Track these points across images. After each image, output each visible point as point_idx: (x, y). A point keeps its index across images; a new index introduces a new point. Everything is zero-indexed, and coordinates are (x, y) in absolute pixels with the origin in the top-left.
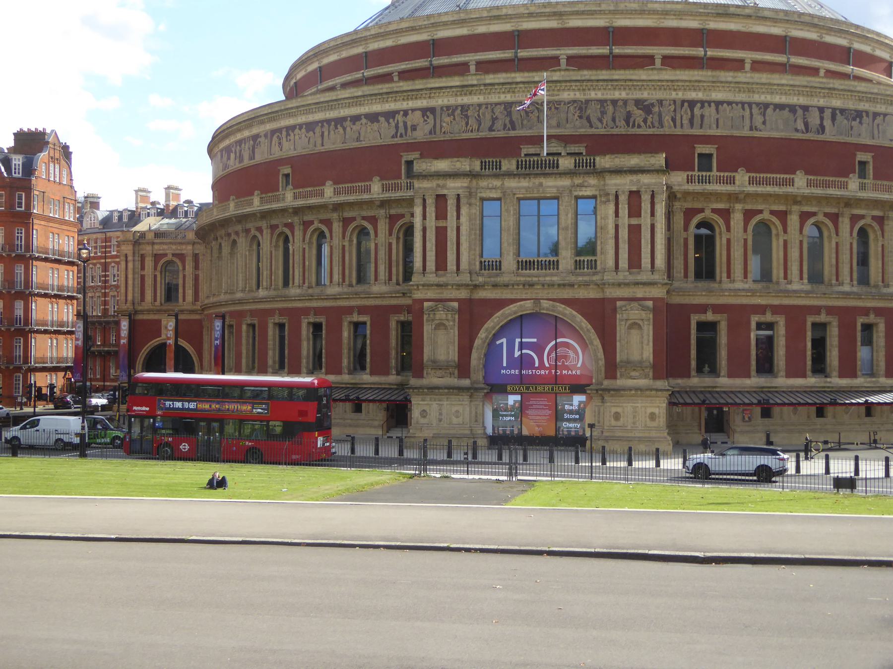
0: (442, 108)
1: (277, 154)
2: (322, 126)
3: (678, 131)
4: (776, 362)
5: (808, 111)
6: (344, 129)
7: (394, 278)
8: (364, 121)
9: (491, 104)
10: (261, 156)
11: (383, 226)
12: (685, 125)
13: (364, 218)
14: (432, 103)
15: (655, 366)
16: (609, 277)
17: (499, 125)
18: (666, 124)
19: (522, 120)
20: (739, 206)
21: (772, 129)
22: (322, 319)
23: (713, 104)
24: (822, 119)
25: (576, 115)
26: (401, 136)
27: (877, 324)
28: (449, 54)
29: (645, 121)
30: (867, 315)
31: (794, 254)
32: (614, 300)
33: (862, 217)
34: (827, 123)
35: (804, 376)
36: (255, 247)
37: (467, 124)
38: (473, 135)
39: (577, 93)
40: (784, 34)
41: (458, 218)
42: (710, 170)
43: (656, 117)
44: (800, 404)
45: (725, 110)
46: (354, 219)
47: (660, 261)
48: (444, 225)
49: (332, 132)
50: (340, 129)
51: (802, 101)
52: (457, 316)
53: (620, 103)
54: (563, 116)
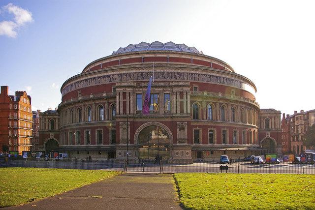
11: (106, 105)
14: (121, 72)
20: (204, 100)
32: (176, 122)
34: (225, 81)
35: (221, 144)
41: (130, 99)
47: (189, 111)
51: (219, 75)
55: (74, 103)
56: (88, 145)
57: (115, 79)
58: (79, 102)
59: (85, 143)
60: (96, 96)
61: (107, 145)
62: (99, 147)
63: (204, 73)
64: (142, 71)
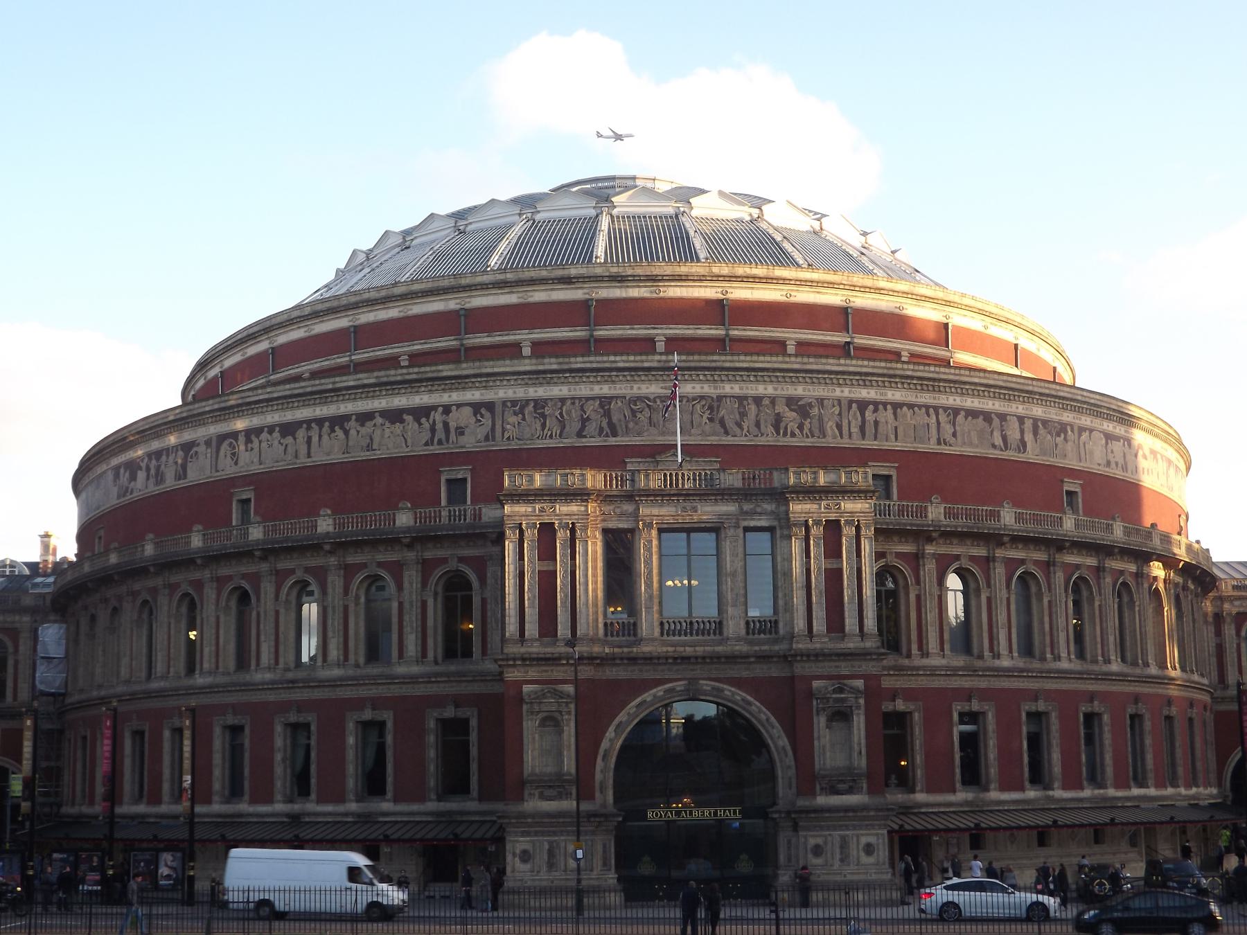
0: (504, 403)
1: (228, 469)
2: (309, 428)
3: (845, 443)
4: (983, 771)
5: (1006, 420)
6: (346, 433)
7: (431, 654)
8: (379, 420)
9: (580, 399)
10: (199, 472)
11: (412, 577)
12: (854, 436)
13: (380, 564)
15: (870, 776)
16: (801, 646)
17: (591, 428)
18: (829, 432)
19: (627, 422)
20: (930, 549)
21: (964, 443)
22: (311, 718)
23: (889, 407)
24: (1022, 432)
26: (440, 442)
27: (1099, 715)
28: (489, 330)
29: (801, 427)
30: (1091, 701)
31: (1002, 617)
32: (809, 679)
33: (1078, 567)
34: (1029, 437)
35: (1022, 789)
36: (184, 610)
37: (544, 426)
38: (552, 443)
39: (706, 386)
40: (945, 321)
42: (888, 496)
43: (815, 421)
44: (1019, 828)
45: (905, 416)
46: (364, 566)
48: (551, 568)
49: (325, 437)
50: (339, 433)
52: (572, 706)
54: (687, 417)
55: (213, 559)
56: (296, 807)
57: (460, 431)
58: (244, 554)
59: (279, 797)
60: (355, 525)
61: (415, 807)
62: (365, 819)
63: (926, 398)
64: (605, 390)
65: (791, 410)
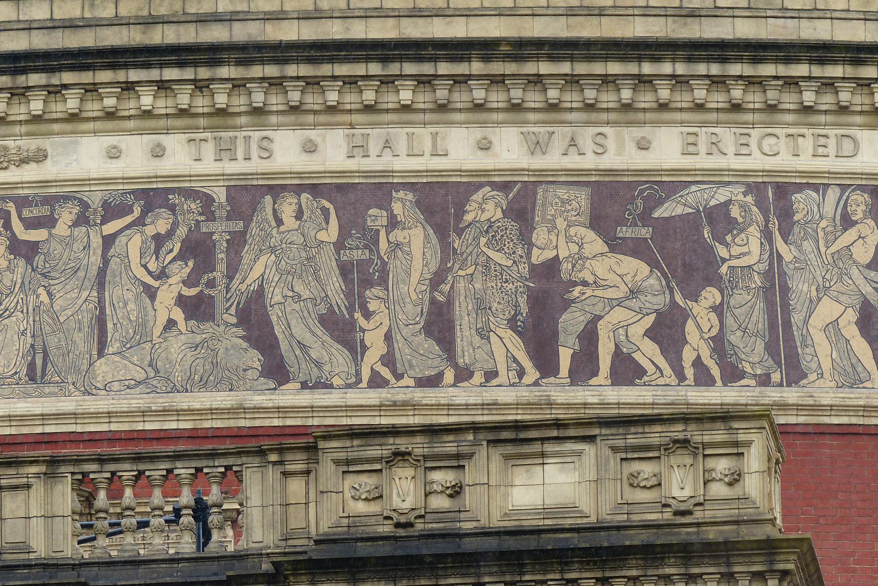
18: (821, 351)
25: (167, 295)
29: (667, 331)
53: (486, 208)
54: (72, 301)
65: (615, 245)
